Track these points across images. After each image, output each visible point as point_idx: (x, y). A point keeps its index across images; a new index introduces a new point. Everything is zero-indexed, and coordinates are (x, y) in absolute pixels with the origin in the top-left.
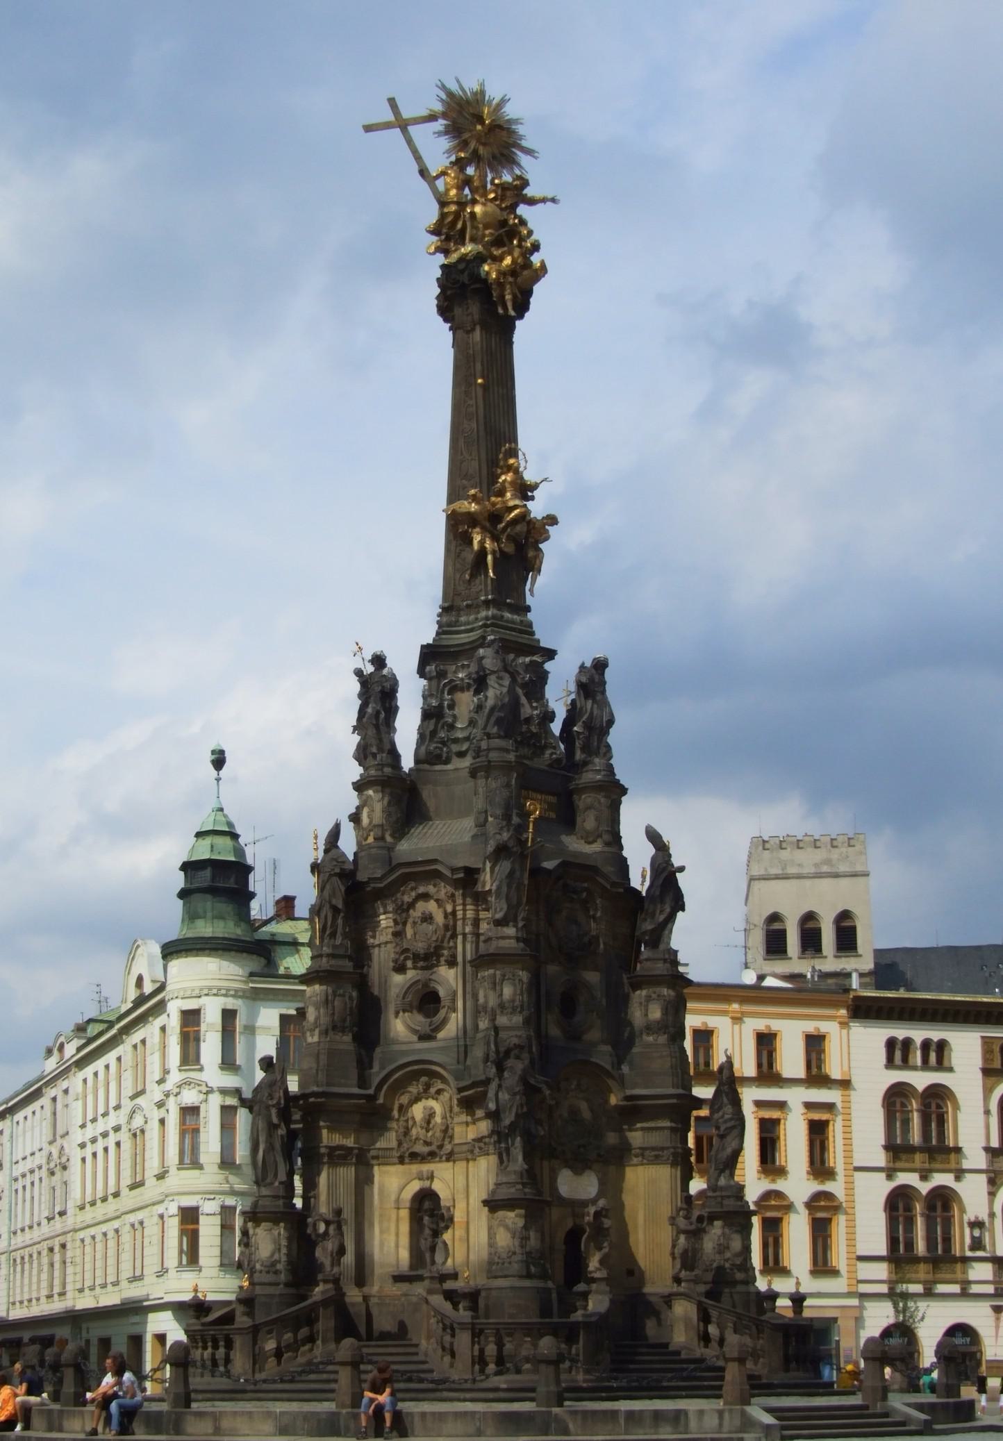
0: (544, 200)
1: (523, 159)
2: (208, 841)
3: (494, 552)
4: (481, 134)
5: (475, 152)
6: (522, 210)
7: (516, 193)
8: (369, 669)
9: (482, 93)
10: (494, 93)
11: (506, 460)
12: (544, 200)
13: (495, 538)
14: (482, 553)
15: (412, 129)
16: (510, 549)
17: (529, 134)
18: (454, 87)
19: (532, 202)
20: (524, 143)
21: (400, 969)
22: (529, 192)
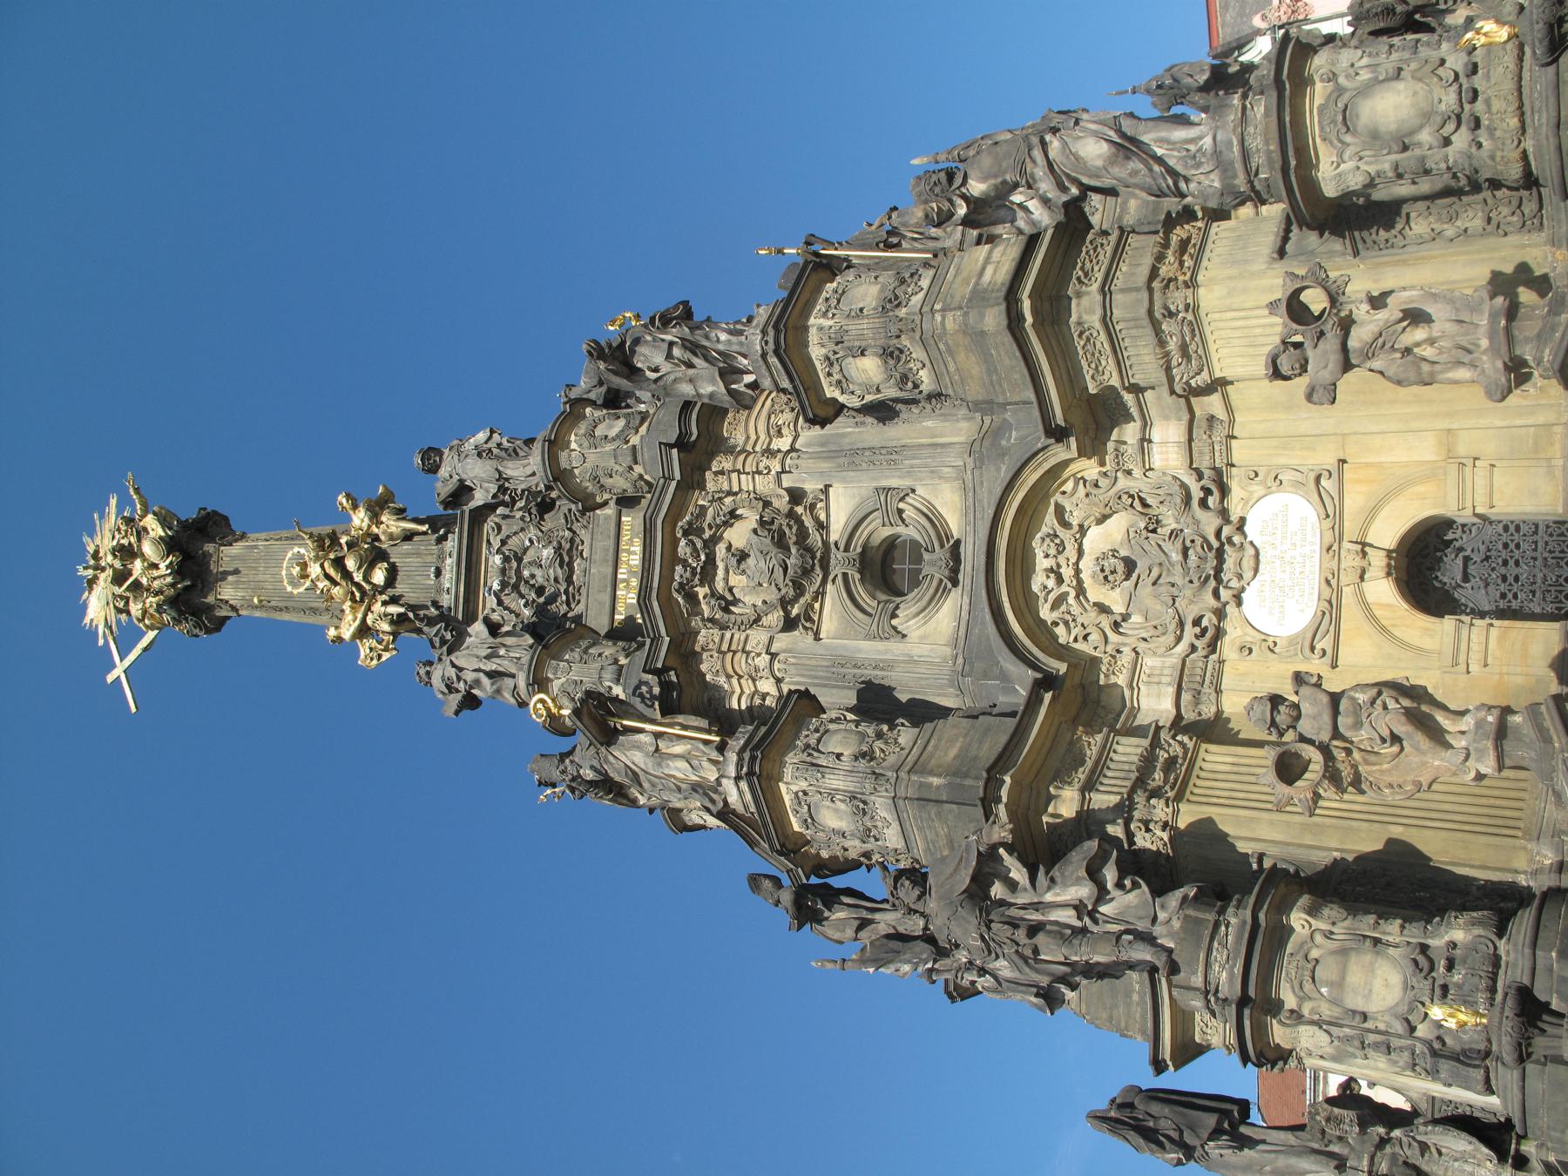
3: (385, 603)
16: (379, 576)
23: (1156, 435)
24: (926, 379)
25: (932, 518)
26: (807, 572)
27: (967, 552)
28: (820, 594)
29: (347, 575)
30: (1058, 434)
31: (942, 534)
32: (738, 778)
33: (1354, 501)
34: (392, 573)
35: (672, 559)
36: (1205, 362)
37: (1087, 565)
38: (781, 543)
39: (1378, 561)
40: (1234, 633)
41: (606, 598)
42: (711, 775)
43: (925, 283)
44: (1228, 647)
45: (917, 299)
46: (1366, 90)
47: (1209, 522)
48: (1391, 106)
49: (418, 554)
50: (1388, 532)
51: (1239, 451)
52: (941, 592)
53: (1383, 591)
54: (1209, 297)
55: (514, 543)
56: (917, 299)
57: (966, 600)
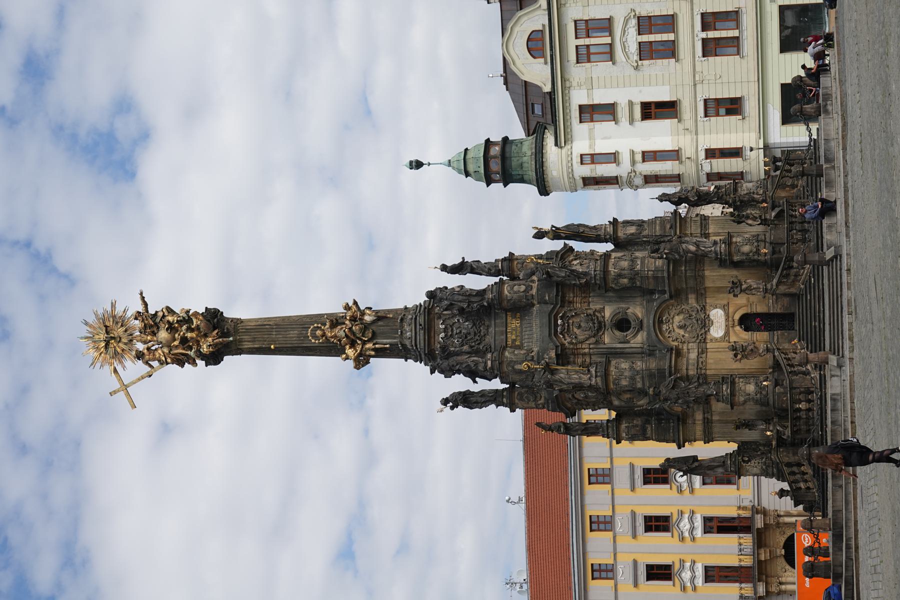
0: (143, 298)
1: (119, 310)
2: (471, 168)
4: (112, 337)
5: (125, 344)
8: (451, 404)
12: (143, 298)
13: (364, 343)
14: (374, 350)
19: (146, 305)
20: (109, 309)
21: (612, 404)
22: (141, 309)
23: (690, 296)
24: (638, 284)
26: (600, 328)
27: (645, 321)
28: (603, 334)
29: (354, 334)
31: (638, 318)
32: (596, 376)
33: (731, 310)
35: (556, 325)
36: (704, 284)
38: (592, 320)
40: (708, 337)
41: (503, 337)
43: (639, 262)
49: (387, 326)
50: (737, 317)
52: (638, 331)
53: (738, 328)
54: (707, 273)
55: (450, 322)
57: (645, 333)
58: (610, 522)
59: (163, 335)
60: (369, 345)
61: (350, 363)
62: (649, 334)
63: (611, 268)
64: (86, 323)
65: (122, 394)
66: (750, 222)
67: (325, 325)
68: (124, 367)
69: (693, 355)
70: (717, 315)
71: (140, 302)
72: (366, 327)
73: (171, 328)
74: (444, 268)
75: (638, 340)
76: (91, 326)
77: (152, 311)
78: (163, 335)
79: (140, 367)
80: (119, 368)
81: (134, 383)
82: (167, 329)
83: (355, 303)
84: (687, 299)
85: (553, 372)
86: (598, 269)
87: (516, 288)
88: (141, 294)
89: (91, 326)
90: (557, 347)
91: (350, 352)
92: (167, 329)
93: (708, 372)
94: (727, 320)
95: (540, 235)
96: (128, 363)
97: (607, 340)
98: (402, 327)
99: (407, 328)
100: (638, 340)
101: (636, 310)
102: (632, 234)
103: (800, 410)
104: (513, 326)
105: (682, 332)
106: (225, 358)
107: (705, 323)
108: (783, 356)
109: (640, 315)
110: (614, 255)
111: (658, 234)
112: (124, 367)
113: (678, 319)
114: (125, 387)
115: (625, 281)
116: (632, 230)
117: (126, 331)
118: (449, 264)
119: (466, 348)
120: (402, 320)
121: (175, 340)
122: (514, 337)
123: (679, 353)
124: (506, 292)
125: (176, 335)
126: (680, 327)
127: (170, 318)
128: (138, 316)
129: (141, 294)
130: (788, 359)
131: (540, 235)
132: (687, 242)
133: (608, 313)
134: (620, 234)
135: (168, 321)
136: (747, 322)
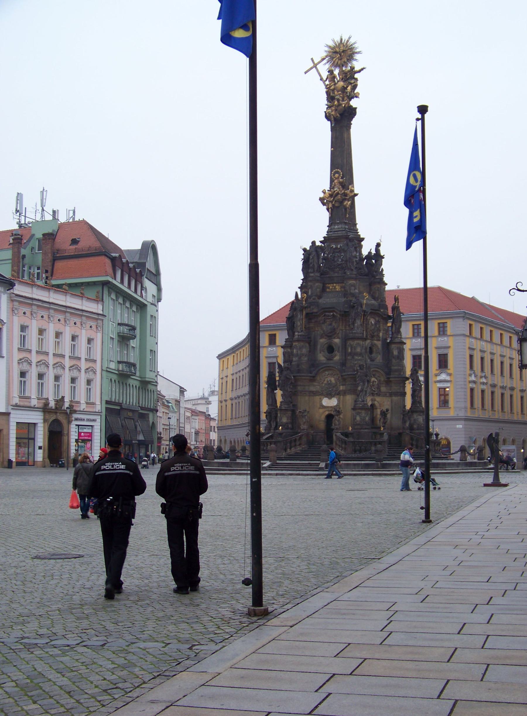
0: (362, 69)
1: (357, 56)
4: (342, 54)
5: (337, 63)
6: (356, 76)
7: (353, 72)
9: (341, 39)
10: (345, 38)
11: (334, 175)
12: (362, 69)
13: (332, 202)
15: (314, 68)
16: (336, 205)
17: (359, 47)
18: (331, 44)
19: (359, 71)
20: (357, 50)
22: (357, 69)
25: (335, 356)
26: (328, 336)
27: (331, 362)
30: (342, 376)
32: (298, 335)
34: (338, 207)
37: (329, 379)
39: (330, 412)
40: (322, 397)
42: (299, 329)
43: (359, 358)
44: (320, 397)
45: (357, 358)
46: (360, 416)
47: (333, 394)
48: (358, 418)
51: (342, 397)
53: (327, 413)
56: (357, 358)
57: (325, 362)
58: (418, 335)
59: (341, 84)
60: (330, 206)
61: (322, 195)
62: (325, 364)
63: (356, 342)
64: (350, 38)
65: (312, 65)
66: (382, 420)
67: (342, 178)
68: (325, 64)
69: (312, 389)
70: (333, 402)
71: (360, 68)
72: (342, 202)
73: (344, 89)
74: (378, 245)
75: (321, 357)
76: (348, 41)
77: (356, 76)
78: (341, 84)
79: (325, 75)
80: (325, 61)
81: (317, 70)
82: (343, 87)
83: (356, 195)
84: (343, 385)
85: (302, 311)
86: (356, 335)
87: (353, 288)
88: (364, 68)
89: (348, 41)
90: (317, 313)
91: (327, 195)
92: (343, 87)
93: (299, 397)
94: (331, 407)
95: (396, 299)
96: (327, 66)
97: (322, 340)
98: (341, 223)
99: (340, 226)
100: (321, 357)
101: (337, 358)
102: (393, 353)
103: (267, 446)
104: (337, 287)
105: (325, 382)
106: (329, 122)
107: (330, 396)
108: (298, 438)
109: (335, 359)
110: (379, 344)
111: (393, 368)
112: (325, 64)
113: (333, 380)
114: (315, 66)
115: (349, 350)
116: (395, 353)
117: (345, 62)
118: (381, 248)
119: (321, 261)
120: (345, 223)
121: (338, 91)
122: (331, 287)
123: (313, 379)
124: (350, 282)
125: (340, 93)
126: (328, 381)
127: (349, 88)
128: (352, 68)
129: (364, 68)
130: (295, 440)
131: (396, 299)
132: (364, 384)
133: (337, 341)
134: (393, 346)
135: (347, 87)
136: (329, 418)
